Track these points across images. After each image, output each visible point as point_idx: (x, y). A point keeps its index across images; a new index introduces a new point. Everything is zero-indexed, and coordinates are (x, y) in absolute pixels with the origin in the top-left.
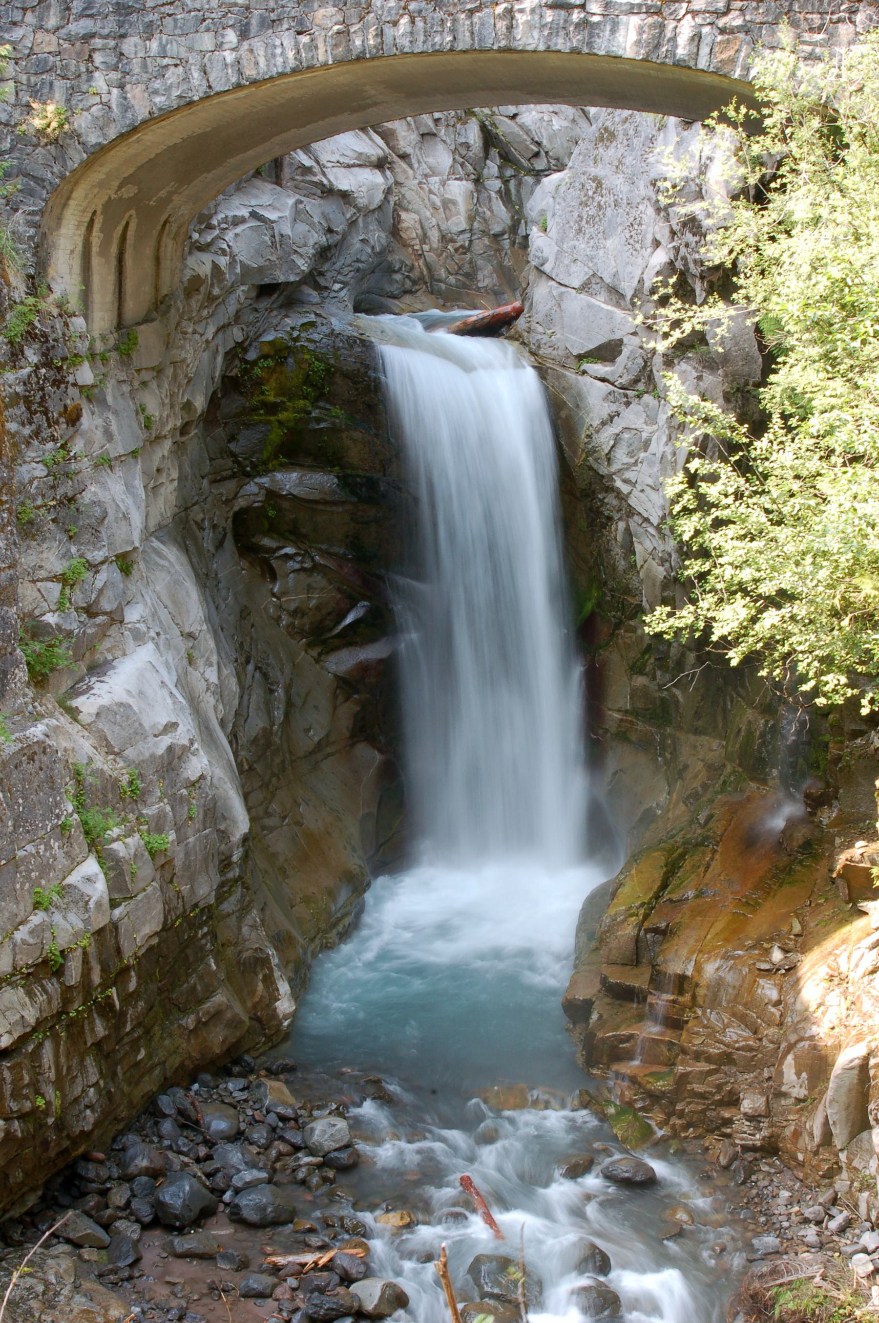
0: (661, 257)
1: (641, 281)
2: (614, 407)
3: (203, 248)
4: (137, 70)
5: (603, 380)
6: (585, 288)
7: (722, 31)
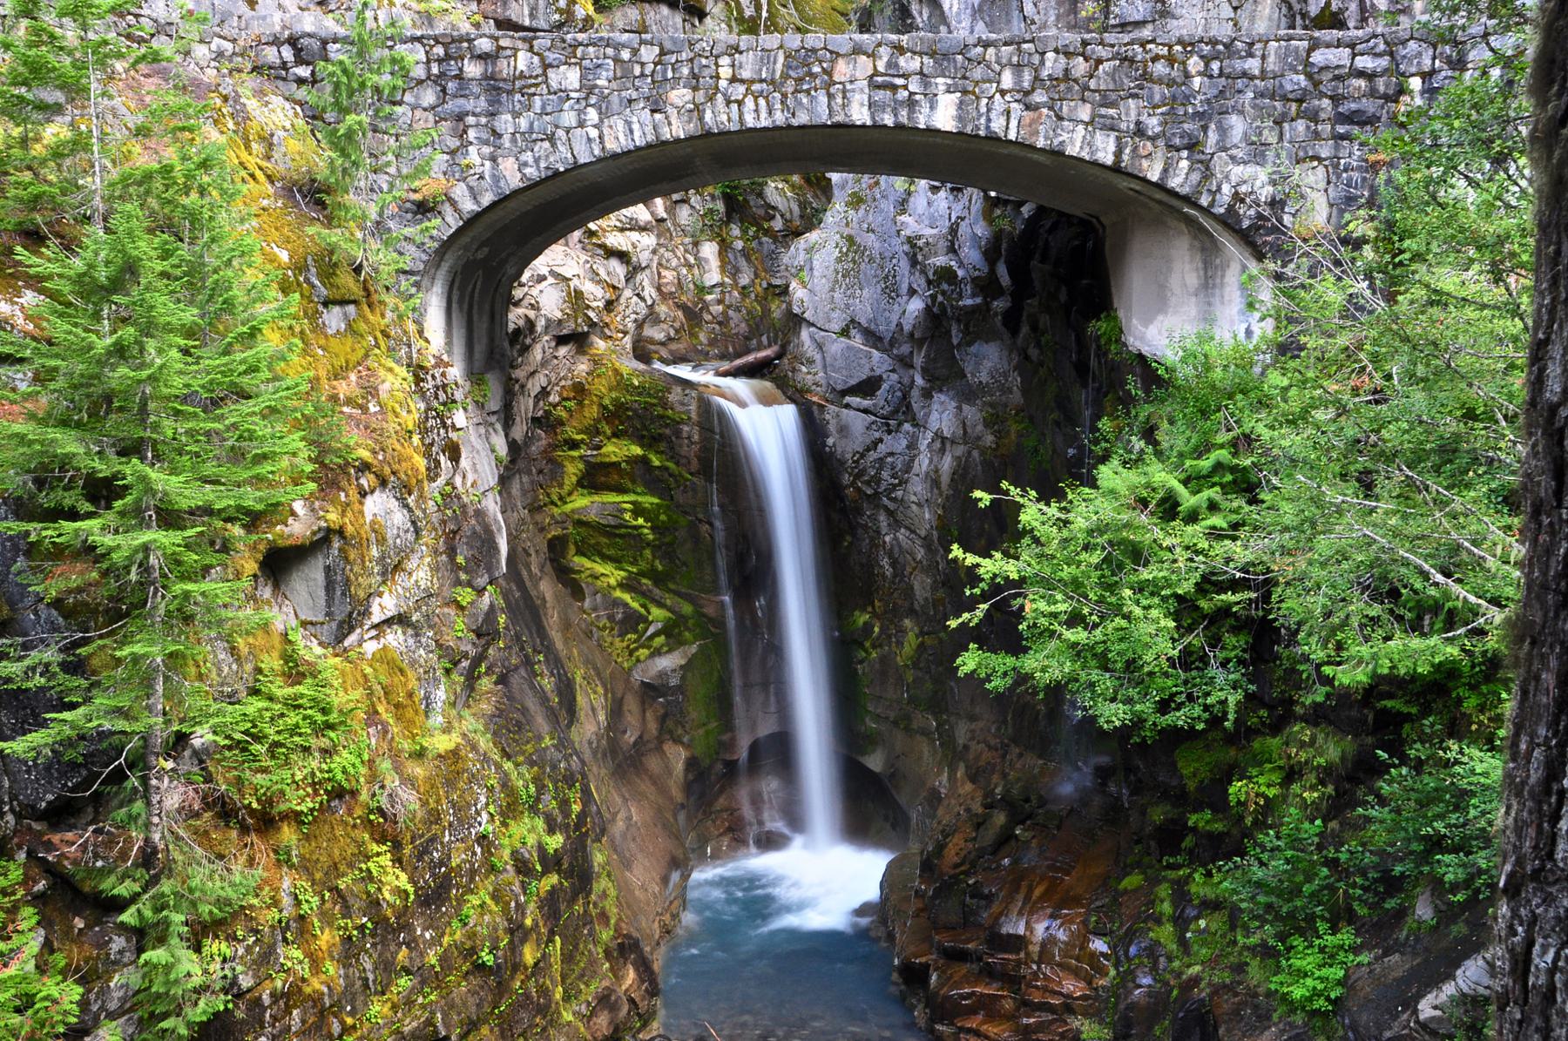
0: (916, 306)
1: (899, 325)
2: (877, 435)
3: (517, 304)
4: (507, 145)
5: (865, 411)
6: (844, 332)
7: (1028, 107)
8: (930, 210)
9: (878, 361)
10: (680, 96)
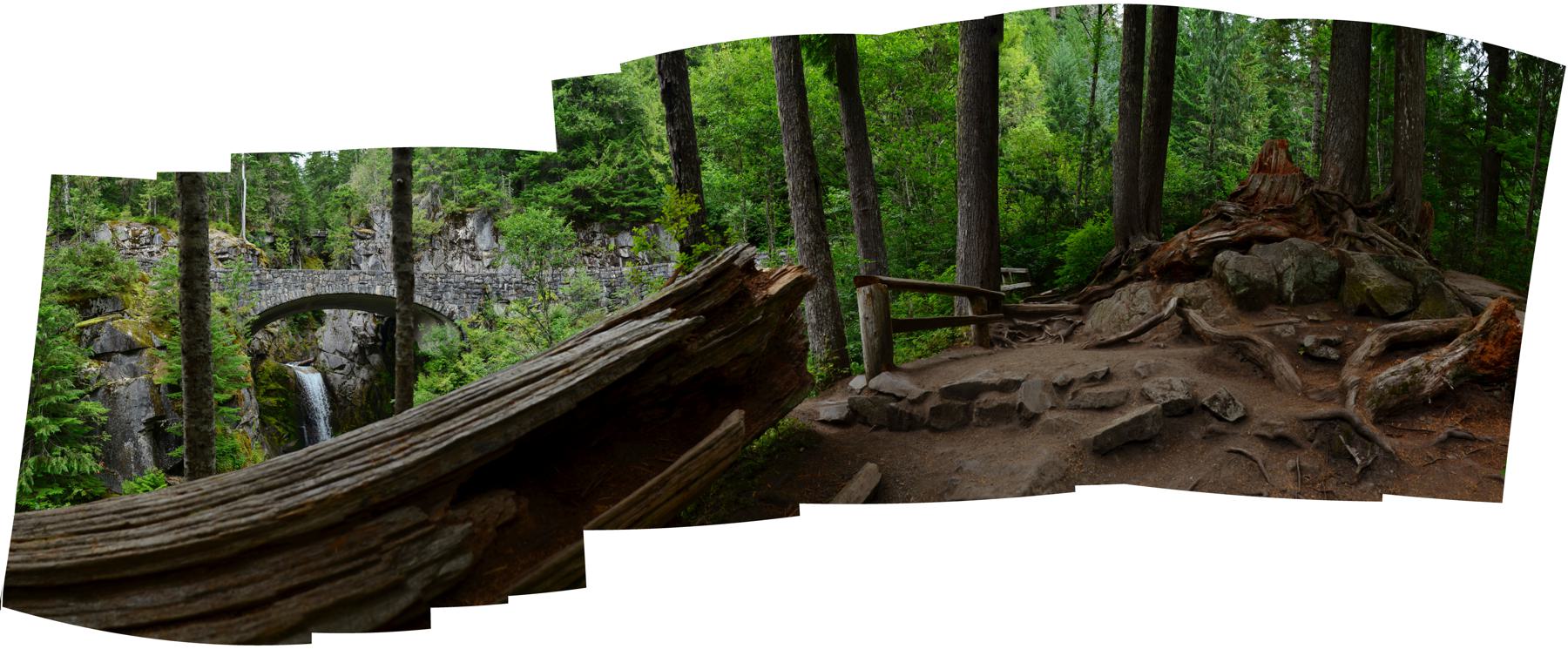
8: (359, 319)
9: (345, 361)
10: (309, 285)
